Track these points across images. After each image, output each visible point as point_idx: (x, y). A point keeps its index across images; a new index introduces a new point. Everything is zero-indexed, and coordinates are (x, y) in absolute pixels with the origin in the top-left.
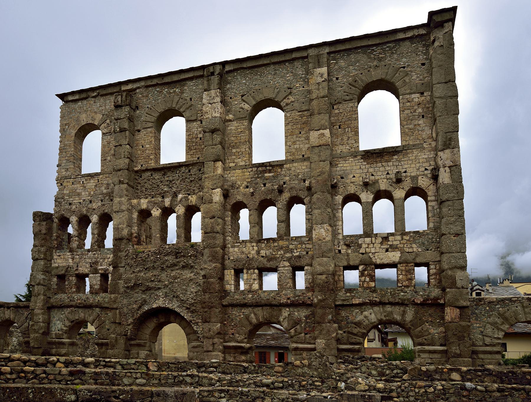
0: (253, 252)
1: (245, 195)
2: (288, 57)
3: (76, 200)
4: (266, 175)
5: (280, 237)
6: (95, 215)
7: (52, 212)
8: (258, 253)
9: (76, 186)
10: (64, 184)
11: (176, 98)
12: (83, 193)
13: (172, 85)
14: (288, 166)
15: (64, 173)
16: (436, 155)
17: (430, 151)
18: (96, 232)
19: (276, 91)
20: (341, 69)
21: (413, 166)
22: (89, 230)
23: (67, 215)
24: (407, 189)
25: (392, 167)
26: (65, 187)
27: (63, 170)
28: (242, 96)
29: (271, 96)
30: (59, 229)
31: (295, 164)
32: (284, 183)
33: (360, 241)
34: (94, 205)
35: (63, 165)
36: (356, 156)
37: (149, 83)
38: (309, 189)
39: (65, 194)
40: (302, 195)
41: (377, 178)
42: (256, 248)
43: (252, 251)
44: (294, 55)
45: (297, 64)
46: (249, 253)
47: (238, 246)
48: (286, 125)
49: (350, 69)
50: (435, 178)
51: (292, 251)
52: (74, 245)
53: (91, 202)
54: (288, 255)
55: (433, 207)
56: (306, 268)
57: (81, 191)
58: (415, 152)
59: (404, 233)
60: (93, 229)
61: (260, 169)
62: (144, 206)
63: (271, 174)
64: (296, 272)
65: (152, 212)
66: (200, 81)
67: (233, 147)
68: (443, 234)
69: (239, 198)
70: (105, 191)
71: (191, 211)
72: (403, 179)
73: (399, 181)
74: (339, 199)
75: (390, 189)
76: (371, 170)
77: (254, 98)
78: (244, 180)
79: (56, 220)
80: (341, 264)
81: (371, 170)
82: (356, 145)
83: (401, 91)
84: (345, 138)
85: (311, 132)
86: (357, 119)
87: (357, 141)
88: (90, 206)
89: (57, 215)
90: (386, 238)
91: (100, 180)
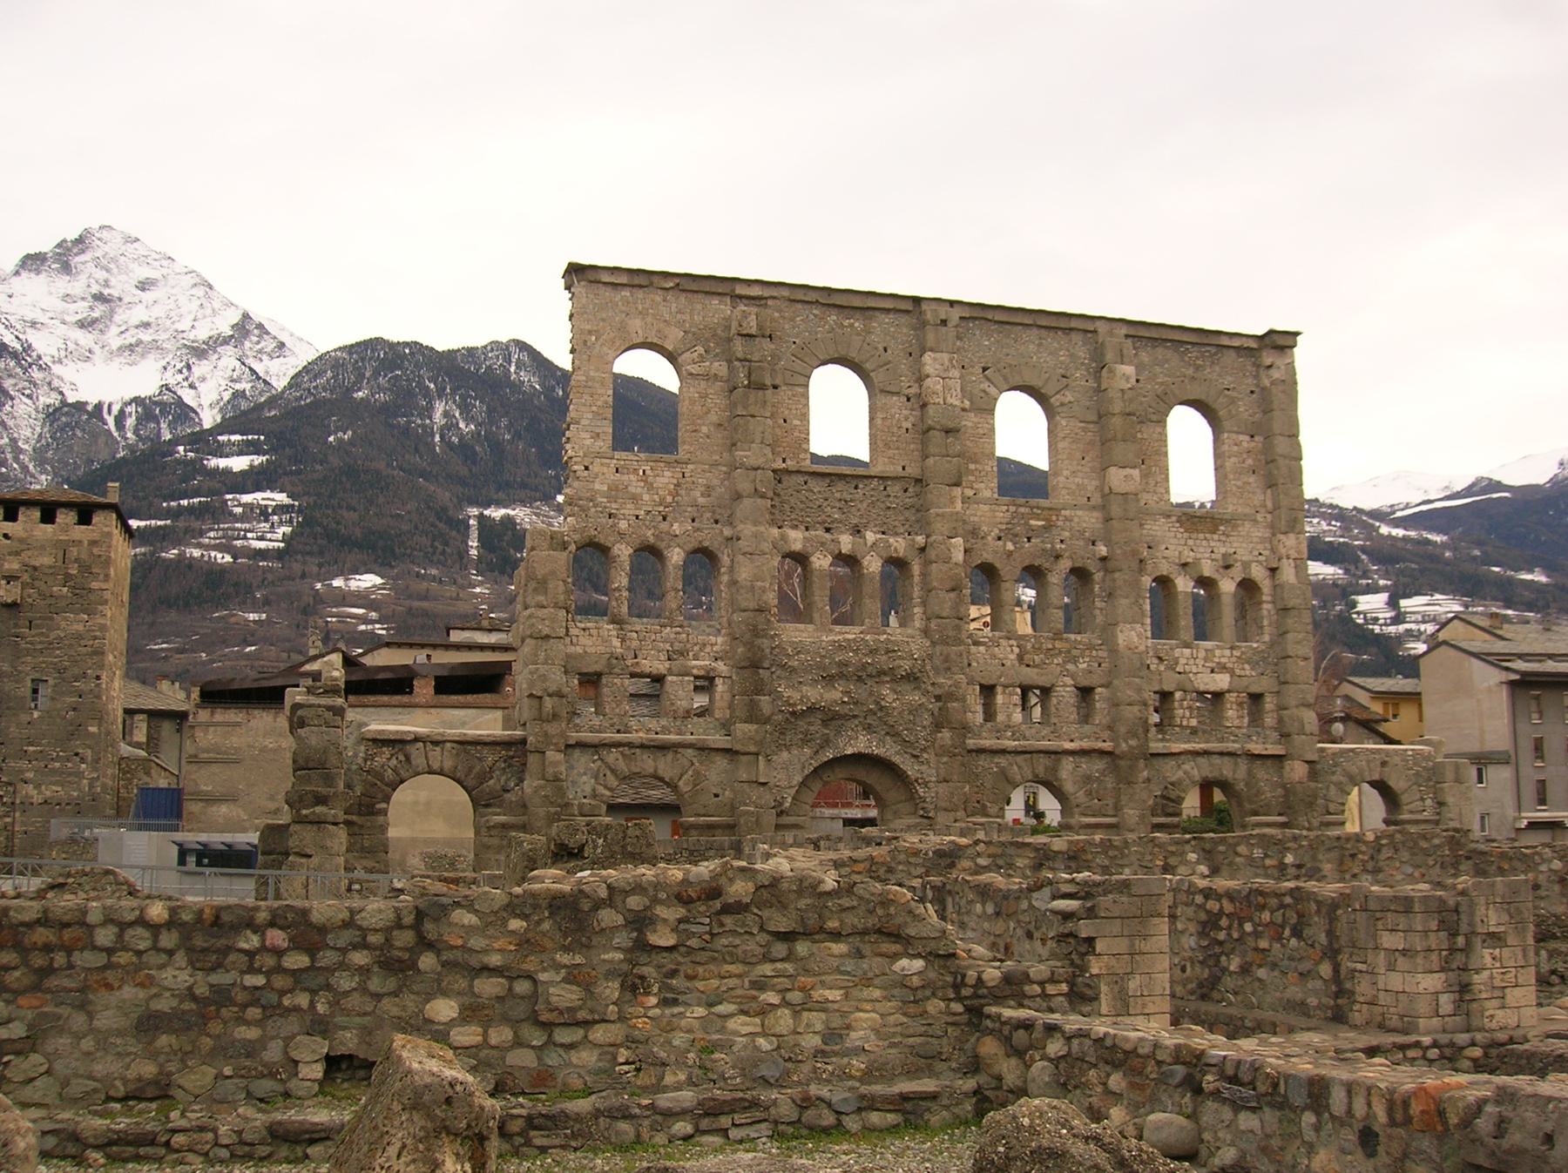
0: (1013, 657)
3: (629, 510)
6: (677, 550)
8: (1020, 658)
10: (595, 468)
12: (646, 497)
13: (846, 311)
14: (1067, 513)
15: (588, 442)
26: (597, 476)
28: (984, 369)
31: (1079, 513)
35: (584, 422)
38: (1103, 559)
39: (597, 492)
40: (1092, 566)
42: (1016, 650)
45: (1077, 338)
65: (813, 559)
66: (904, 319)
73: (1227, 567)
75: (1215, 576)
81: (1190, 542)
83: (1227, 424)
86: (1166, 454)
87: (1168, 492)
89: (577, 537)
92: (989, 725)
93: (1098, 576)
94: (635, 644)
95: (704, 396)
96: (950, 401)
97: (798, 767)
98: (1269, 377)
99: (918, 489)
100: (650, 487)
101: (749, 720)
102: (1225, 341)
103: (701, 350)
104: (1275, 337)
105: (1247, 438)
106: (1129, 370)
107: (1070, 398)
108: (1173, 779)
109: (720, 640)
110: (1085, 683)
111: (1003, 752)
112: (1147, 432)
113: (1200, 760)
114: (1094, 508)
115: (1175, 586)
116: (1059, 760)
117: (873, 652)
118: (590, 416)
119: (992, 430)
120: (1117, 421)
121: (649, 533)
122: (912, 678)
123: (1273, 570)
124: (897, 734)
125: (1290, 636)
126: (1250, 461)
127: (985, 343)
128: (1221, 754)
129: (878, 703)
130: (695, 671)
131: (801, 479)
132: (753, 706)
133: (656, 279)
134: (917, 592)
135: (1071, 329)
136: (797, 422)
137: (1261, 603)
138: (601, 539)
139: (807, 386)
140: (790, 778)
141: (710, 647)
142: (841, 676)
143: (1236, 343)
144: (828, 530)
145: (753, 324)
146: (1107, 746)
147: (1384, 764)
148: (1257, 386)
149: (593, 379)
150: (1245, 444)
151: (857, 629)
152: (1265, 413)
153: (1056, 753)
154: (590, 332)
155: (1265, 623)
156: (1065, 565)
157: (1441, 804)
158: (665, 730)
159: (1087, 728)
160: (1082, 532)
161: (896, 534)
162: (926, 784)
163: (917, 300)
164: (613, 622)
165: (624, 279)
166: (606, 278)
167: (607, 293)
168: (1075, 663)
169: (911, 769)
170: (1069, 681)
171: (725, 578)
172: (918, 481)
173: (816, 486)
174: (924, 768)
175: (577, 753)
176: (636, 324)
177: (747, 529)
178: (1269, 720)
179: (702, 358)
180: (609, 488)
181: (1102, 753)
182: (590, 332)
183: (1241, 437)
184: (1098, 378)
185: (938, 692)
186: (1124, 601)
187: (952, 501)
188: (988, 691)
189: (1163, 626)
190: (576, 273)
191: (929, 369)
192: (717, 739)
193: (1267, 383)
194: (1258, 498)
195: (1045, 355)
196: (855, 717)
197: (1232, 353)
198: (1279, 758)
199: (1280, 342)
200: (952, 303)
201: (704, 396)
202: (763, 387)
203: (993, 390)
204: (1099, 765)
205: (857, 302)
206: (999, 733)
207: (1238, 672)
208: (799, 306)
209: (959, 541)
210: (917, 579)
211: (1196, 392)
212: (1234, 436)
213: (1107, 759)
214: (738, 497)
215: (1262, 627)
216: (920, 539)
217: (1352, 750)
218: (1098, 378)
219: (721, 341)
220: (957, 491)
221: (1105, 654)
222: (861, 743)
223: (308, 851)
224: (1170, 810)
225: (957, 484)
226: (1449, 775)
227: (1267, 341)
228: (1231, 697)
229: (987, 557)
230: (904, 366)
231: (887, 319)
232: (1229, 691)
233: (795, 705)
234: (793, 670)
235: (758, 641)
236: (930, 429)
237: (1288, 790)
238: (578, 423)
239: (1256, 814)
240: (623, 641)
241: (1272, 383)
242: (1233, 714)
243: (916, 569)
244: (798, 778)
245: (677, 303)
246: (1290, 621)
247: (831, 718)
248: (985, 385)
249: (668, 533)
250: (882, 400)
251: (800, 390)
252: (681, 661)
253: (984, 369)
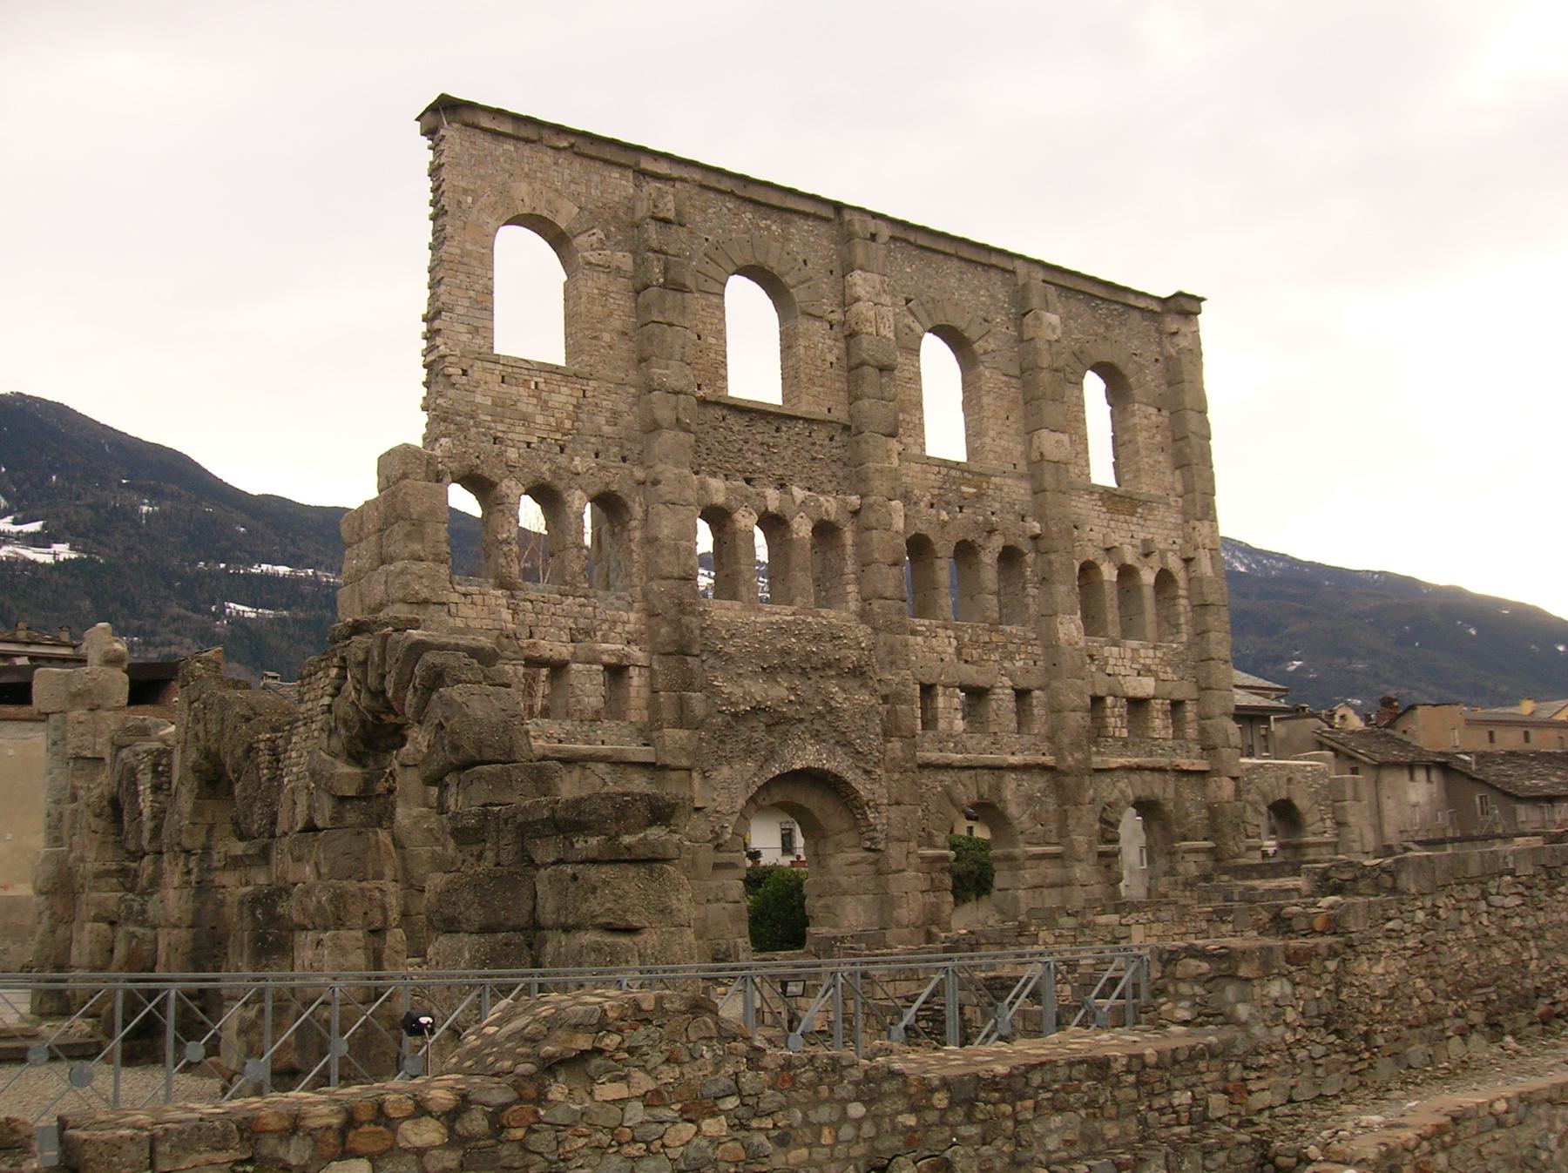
0: (951, 650)
2: (983, 258)
4: (964, 489)
9: (514, 390)
10: (476, 373)
12: (540, 419)
13: (763, 210)
27: (463, 329)
28: (908, 301)
31: (1009, 481)
36: (1091, 493)
38: (1035, 538)
39: (479, 406)
40: (1025, 545)
42: (954, 642)
45: (995, 276)
53: (562, 451)
57: (531, 409)
61: (953, 473)
62: (719, 499)
63: (973, 490)
65: (737, 516)
66: (823, 229)
73: (1147, 555)
75: (1137, 565)
89: (454, 466)
91: (588, 394)
92: (930, 734)
93: (1030, 557)
94: (530, 617)
95: (605, 294)
96: (884, 332)
97: (742, 785)
98: (1174, 345)
99: (845, 438)
100: (544, 406)
101: (680, 723)
102: (1132, 301)
104: (1183, 300)
105: (1153, 410)
106: (1054, 319)
107: (992, 346)
108: (1111, 799)
109: (633, 616)
110: (1023, 684)
111: (948, 767)
112: (1070, 391)
113: (1135, 777)
114: (1021, 477)
115: (1099, 573)
116: (1002, 777)
117: (817, 638)
118: (466, 303)
119: (919, 374)
120: (1045, 376)
121: (545, 467)
122: (858, 672)
123: (1187, 561)
124: (850, 744)
125: (1212, 635)
128: (1153, 770)
129: (825, 703)
130: (605, 658)
131: (719, 413)
132: (682, 705)
133: (546, 134)
134: (850, 567)
135: (992, 266)
136: (712, 340)
137: (1176, 597)
138: (485, 471)
139: (723, 296)
140: (732, 801)
141: (621, 629)
142: (784, 667)
143: (1142, 304)
144: (748, 481)
145: (671, 205)
146: (1049, 760)
148: (1161, 354)
149: (470, 254)
151: (789, 609)
152: (1170, 384)
153: (999, 768)
154: (466, 191)
155: (1182, 620)
156: (997, 542)
157: (1340, 824)
158: (571, 737)
159: (1026, 739)
160: (1012, 505)
161: (823, 492)
163: (838, 207)
164: (501, 586)
165: (507, 128)
166: (486, 122)
167: (485, 143)
168: (1012, 659)
169: (863, 787)
170: (1007, 681)
171: (637, 535)
172: (846, 428)
174: (876, 786)
176: (521, 189)
177: (667, 471)
178: (1191, 732)
179: (602, 245)
180: (495, 404)
181: (1044, 768)
182: (466, 191)
184: (1019, 326)
185: (885, 690)
186: (1062, 588)
188: (927, 690)
189: (1092, 622)
190: (445, 114)
191: (860, 291)
192: (636, 751)
193: (1173, 351)
194: (1168, 479)
195: (971, 297)
196: (801, 720)
197: (1136, 314)
198: (1201, 774)
199: (1185, 306)
200: (875, 216)
201: (605, 294)
202: (681, 288)
203: (917, 327)
204: (1038, 784)
205: (775, 200)
206: (941, 743)
208: (712, 195)
210: (849, 550)
211: (1106, 354)
212: (1144, 408)
213: (1047, 776)
214: (654, 427)
215: (1177, 626)
216: (854, 500)
217: (1262, 766)
218: (1019, 326)
219: (629, 228)
220: (894, 445)
221: (1038, 650)
222: (808, 756)
223: (634, 920)
224: (1110, 836)
225: (892, 435)
226: (1349, 794)
227: (1171, 304)
228: (1157, 704)
229: (922, 527)
230: (825, 285)
231: (806, 225)
232: (1154, 698)
233: (738, 704)
234: (730, 659)
235: (685, 620)
236: (863, 364)
237: (1214, 811)
238: (451, 310)
239: (1185, 839)
240: (515, 612)
241: (1178, 352)
242: (1159, 724)
243: (848, 537)
244: (741, 802)
245: (568, 170)
246: (1210, 619)
247: (776, 720)
248: (909, 320)
249: (567, 470)
250: (804, 324)
251: (715, 300)
252: (587, 643)
253: (908, 301)
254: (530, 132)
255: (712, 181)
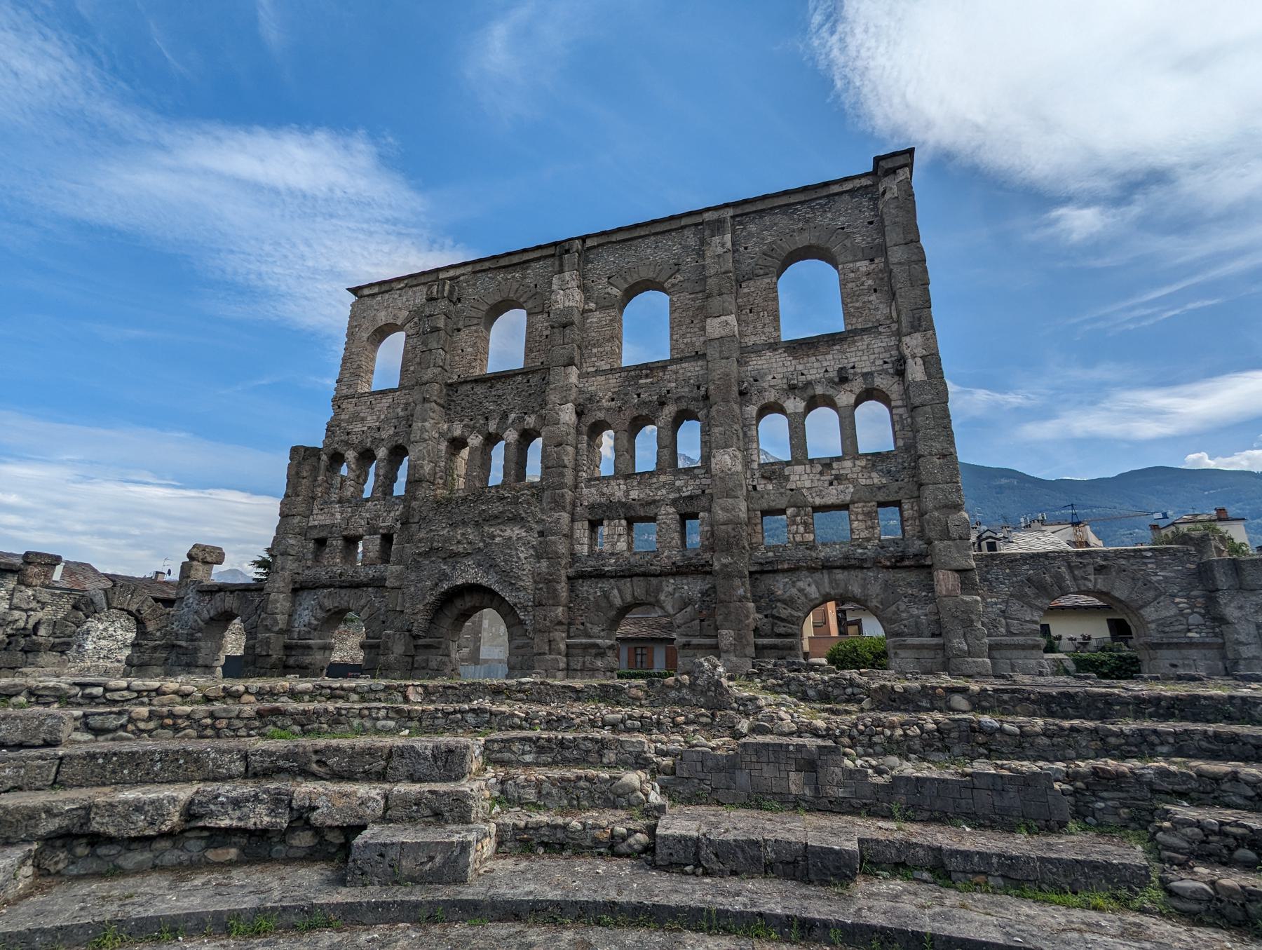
1: (608, 410)
3: (358, 428)
5: (660, 469)
7: (321, 446)
8: (627, 494)
10: (343, 406)
11: (515, 286)
16: (900, 341)
17: (889, 336)
18: (382, 472)
19: (658, 268)
20: (751, 235)
21: (865, 358)
22: (372, 470)
23: (341, 449)
24: (858, 391)
25: (831, 361)
29: (651, 275)
30: (328, 470)
32: (668, 392)
33: (787, 471)
34: (384, 435)
36: (775, 350)
37: (478, 267)
38: (706, 397)
41: (809, 378)
43: (618, 491)
44: (684, 222)
45: (687, 232)
46: (613, 495)
47: (594, 486)
48: (672, 312)
49: (765, 235)
50: (901, 373)
51: (679, 490)
52: (349, 492)
54: (672, 496)
55: (901, 416)
56: (701, 514)
58: (867, 339)
59: (856, 456)
60: (377, 468)
62: (457, 432)
64: (687, 522)
66: (549, 261)
67: (594, 346)
68: (920, 456)
69: (601, 415)
70: (401, 414)
71: (527, 436)
72: (851, 377)
74: (752, 410)
75: (831, 392)
76: (800, 367)
77: (625, 280)
78: (609, 390)
79: (324, 457)
80: (757, 507)
82: (775, 334)
83: (841, 259)
84: (759, 325)
85: (709, 320)
87: (777, 329)
88: (377, 435)
90: (827, 464)
95: (414, 348)
96: (567, 304)
102: (836, 189)
103: (416, 320)
104: (882, 163)
105: (867, 263)
113: (817, 575)
126: (870, 282)
127: (608, 261)
131: (469, 387)
133: (393, 285)
135: (683, 228)
142: (464, 523)
147: (1100, 570)
150: (864, 269)
162: (525, 608)
165: (376, 290)
170: (672, 510)
173: (480, 389)
174: (521, 594)
175: (305, 594)
183: (858, 264)
187: (567, 376)
197: (846, 197)
205: (516, 259)
207: (863, 482)
209: (570, 406)
224: (781, 630)
232: (853, 502)
254: (385, 286)
255: (478, 267)
